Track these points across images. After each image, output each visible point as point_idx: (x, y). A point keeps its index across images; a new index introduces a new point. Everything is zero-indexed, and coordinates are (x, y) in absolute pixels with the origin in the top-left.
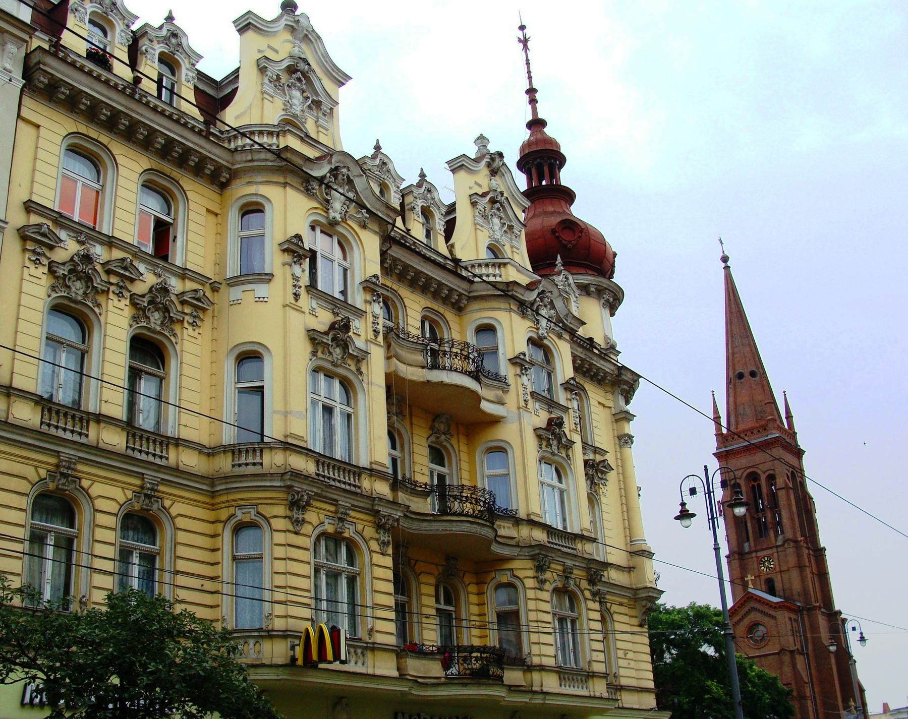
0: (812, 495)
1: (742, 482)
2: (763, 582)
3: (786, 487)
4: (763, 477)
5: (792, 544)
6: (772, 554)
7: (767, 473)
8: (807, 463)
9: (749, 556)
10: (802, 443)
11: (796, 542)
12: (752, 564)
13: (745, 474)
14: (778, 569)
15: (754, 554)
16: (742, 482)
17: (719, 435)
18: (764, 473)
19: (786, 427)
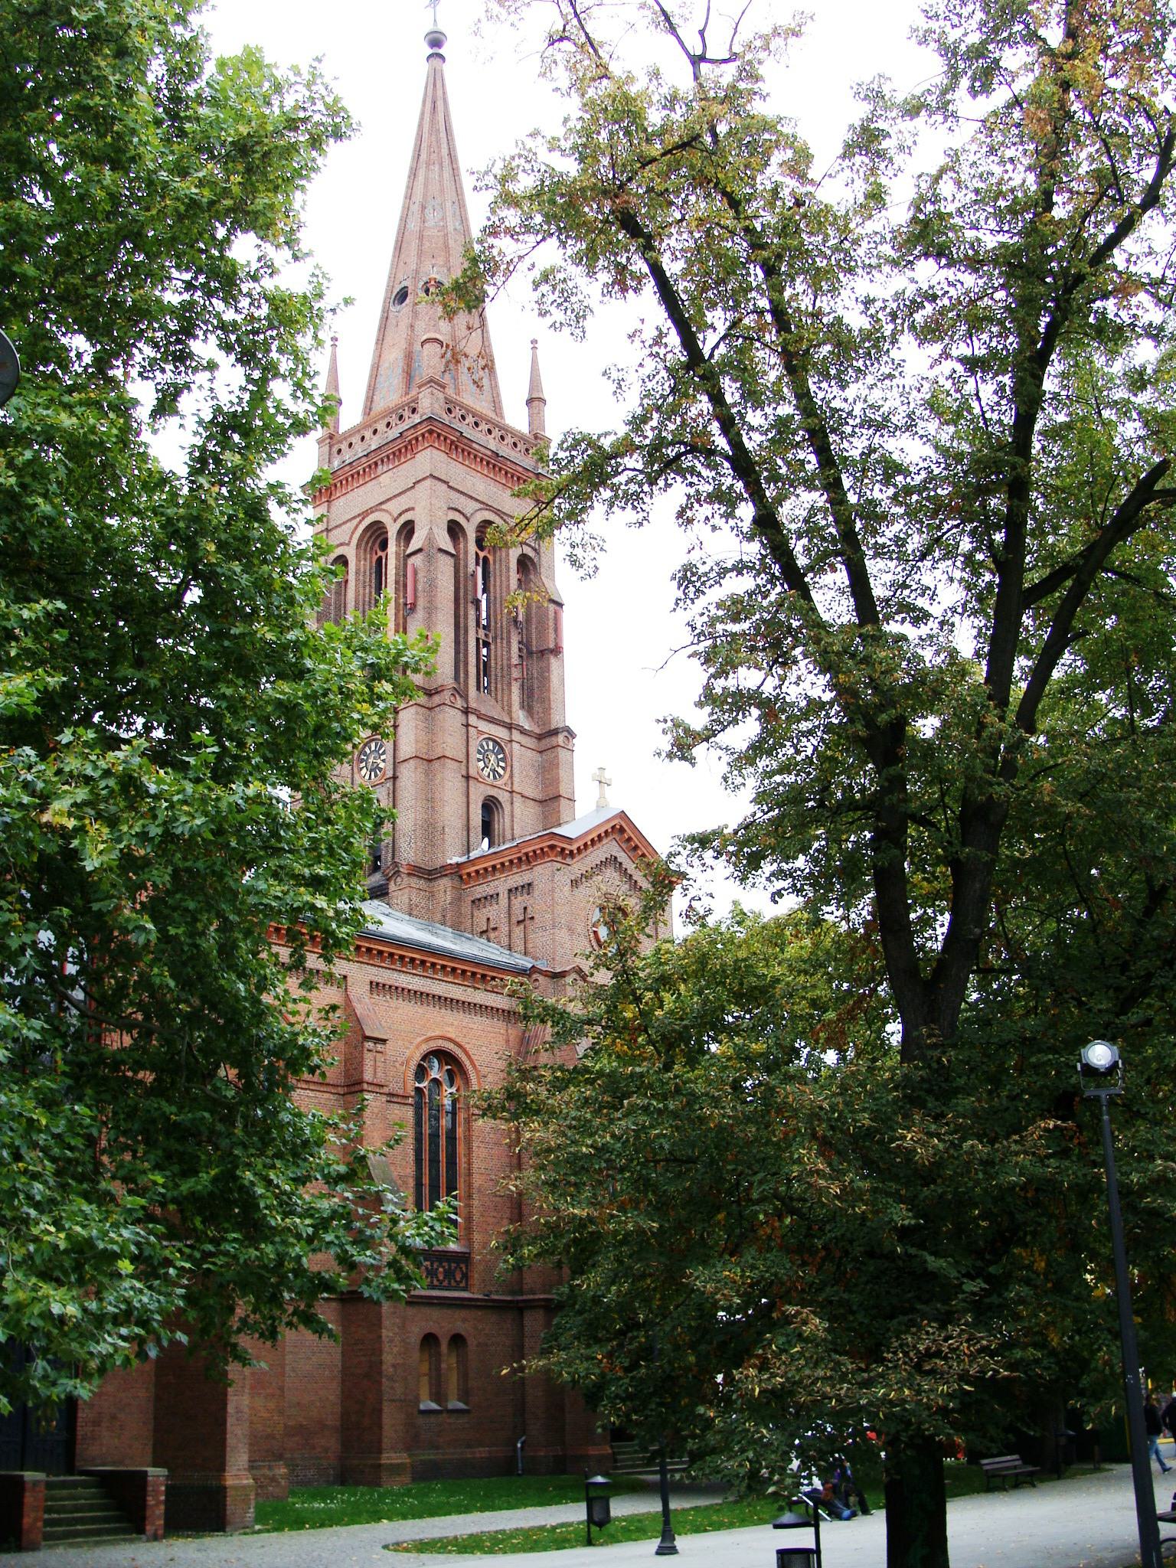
1: (350, 552)
3: (428, 551)
14: (390, 774)
16: (350, 552)
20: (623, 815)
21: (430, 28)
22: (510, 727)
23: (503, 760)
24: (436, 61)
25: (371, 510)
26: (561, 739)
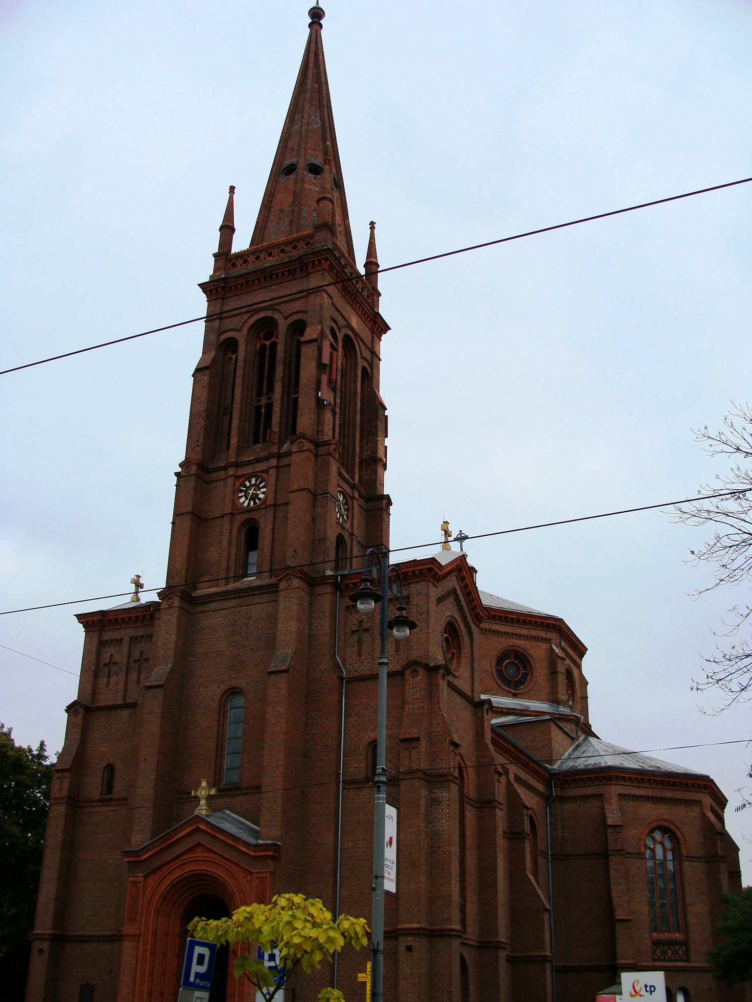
0: (386, 403)
4: (283, 325)
5: (307, 445)
6: (266, 471)
7: (291, 320)
8: (387, 345)
9: (222, 474)
11: (318, 444)
15: (231, 471)
16: (241, 337)
18: (286, 318)
21: (314, 4)
22: (353, 487)
24: (316, 27)
26: (385, 502)
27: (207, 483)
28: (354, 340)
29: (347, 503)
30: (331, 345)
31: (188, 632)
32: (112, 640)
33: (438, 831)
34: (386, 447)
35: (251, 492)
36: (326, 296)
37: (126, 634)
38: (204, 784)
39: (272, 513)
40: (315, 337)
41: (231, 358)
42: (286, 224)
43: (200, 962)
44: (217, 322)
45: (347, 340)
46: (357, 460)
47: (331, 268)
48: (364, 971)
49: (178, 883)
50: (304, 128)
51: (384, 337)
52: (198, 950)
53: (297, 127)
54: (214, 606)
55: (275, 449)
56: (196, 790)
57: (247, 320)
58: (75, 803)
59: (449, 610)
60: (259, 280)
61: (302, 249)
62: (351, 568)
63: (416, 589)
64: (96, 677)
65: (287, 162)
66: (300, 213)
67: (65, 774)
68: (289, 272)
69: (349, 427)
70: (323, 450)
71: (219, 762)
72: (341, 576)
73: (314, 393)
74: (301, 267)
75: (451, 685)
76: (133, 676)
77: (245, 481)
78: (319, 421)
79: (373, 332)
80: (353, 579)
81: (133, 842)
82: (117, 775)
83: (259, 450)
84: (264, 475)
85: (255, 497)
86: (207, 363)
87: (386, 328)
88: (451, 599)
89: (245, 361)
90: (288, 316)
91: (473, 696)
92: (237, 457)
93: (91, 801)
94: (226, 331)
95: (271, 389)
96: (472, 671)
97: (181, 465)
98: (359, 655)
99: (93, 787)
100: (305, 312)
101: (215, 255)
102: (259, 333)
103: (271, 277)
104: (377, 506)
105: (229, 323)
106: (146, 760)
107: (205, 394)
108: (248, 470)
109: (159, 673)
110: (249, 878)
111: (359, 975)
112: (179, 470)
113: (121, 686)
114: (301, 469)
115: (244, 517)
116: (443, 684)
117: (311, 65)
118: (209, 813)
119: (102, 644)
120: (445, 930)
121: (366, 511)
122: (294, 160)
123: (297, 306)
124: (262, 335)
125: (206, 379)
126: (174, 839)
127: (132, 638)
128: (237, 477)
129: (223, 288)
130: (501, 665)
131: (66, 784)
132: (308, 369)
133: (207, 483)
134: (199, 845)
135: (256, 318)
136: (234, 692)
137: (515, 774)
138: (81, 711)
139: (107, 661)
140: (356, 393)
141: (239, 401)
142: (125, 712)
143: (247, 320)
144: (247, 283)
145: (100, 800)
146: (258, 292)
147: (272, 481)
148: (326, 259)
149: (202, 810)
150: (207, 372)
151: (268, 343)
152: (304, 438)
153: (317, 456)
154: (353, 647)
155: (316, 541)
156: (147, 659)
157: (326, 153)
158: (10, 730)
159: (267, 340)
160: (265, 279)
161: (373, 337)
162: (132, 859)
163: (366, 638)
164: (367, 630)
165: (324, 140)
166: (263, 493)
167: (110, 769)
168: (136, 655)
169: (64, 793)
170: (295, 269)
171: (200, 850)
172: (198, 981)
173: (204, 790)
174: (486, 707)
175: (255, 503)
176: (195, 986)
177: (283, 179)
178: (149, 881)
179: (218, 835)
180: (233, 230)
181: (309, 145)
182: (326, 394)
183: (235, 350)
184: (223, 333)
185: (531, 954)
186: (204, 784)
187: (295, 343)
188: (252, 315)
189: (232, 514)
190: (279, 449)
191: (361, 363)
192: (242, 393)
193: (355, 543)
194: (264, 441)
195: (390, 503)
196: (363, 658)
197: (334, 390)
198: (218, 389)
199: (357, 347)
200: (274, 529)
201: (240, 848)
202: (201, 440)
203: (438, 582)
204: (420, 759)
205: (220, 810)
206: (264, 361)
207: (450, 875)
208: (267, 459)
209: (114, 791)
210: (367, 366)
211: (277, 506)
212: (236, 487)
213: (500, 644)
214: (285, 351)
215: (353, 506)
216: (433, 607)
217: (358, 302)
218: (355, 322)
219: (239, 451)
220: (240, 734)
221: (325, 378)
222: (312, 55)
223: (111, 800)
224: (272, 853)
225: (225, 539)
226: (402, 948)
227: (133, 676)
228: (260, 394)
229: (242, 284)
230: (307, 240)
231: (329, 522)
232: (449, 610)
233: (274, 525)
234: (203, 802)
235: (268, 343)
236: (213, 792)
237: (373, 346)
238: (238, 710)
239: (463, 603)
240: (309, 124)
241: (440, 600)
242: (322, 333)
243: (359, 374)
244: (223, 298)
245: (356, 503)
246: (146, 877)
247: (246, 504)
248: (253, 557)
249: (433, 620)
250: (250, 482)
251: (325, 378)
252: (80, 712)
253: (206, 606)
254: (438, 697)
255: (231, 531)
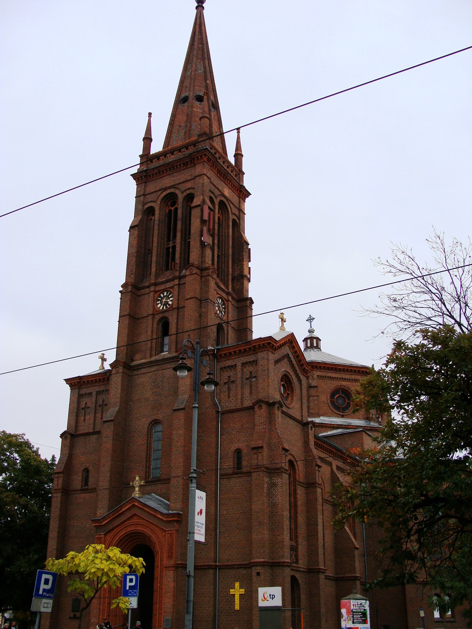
1: (157, 206)
2: (155, 323)
4: (181, 197)
5: (195, 271)
6: (172, 287)
7: (185, 194)
8: (249, 205)
9: (147, 290)
10: (247, 183)
11: (202, 270)
12: (147, 301)
13: (162, 196)
15: (152, 288)
16: (157, 206)
17: (146, 157)
18: (182, 193)
19: (232, 160)
20: (292, 335)
22: (228, 294)
23: (224, 308)
24: (200, 8)
25: (170, 187)
26: (248, 302)
27: (138, 296)
28: (227, 203)
29: (224, 304)
30: (209, 208)
31: (128, 388)
32: (86, 394)
33: (276, 503)
34: (250, 268)
35: (164, 300)
36: (205, 178)
37: (94, 390)
38: (137, 478)
39: (176, 313)
40: (199, 203)
41: (151, 219)
42: (183, 134)
43: (47, 581)
44: (142, 197)
45: (222, 203)
46: (230, 277)
47: (209, 160)
48: (234, 588)
49: (124, 537)
50: (193, 73)
51: (247, 200)
52: (44, 576)
53: (189, 73)
54: (143, 371)
55: (177, 274)
56: (133, 482)
57: (160, 195)
58: (66, 492)
59: (285, 367)
60: (166, 170)
61: (191, 150)
62: (228, 344)
63: (261, 355)
64: (77, 416)
65: (183, 95)
66: (190, 127)
67: (60, 475)
68: (184, 164)
69: (225, 257)
70: (205, 273)
71: (148, 465)
72: (217, 349)
73: (199, 239)
74: (189, 162)
75: (283, 412)
76: (99, 415)
77: (160, 294)
78: (203, 255)
79: (239, 197)
80: (224, 351)
81: (98, 515)
82: (91, 474)
83: (168, 275)
84: (171, 290)
85: (166, 303)
86: (136, 224)
87: (248, 194)
88: (286, 360)
89: (159, 221)
90: (184, 192)
91: (302, 419)
92: (156, 279)
93: (75, 491)
94: (148, 203)
95: (175, 237)
96: (302, 404)
97: (122, 286)
98: (229, 397)
99: (77, 482)
100: (194, 188)
101: (141, 156)
102: (167, 203)
103: (173, 168)
104: (244, 305)
105: (149, 198)
106: (104, 465)
107: (136, 242)
108: (162, 287)
109: (111, 413)
110: (164, 534)
111: (231, 590)
112: (121, 289)
113: (92, 421)
114: (192, 285)
115: (161, 315)
116: (278, 414)
117: (197, 33)
118: (141, 496)
119: (80, 396)
120: (280, 562)
121: (237, 308)
122: (187, 94)
123: (189, 185)
124: (169, 204)
125: (136, 232)
126: (121, 512)
127: (97, 392)
128: (156, 292)
129: (145, 176)
130: (333, 398)
131: (61, 481)
132: (195, 224)
133: (138, 296)
134: (135, 515)
135: (165, 193)
136: (156, 422)
137: (337, 466)
138: (69, 437)
139: (84, 406)
140: (228, 236)
141: (156, 245)
142: (94, 436)
143: (160, 195)
144: (160, 172)
145: (81, 490)
146: (166, 177)
147: (176, 293)
148: (205, 155)
149: (136, 494)
150: (137, 228)
151: (173, 209)
152: (193, 266)
153: (201, 277)
154: (225, 392)
155: (202, 329)
156: (106, 404)
157: (207, 87)
158: (38, 449)
159: (172, 206)
160: (170, 169)
161: (239, 200)
162: (97, 524)
163: (233, 387)
164: (233, 382)
165: (206, 80)
166: (171, 301)
167: (86, 471)
168: (100, 402)
169: (60, 486)
170: (187, 162)
171: (136, 518)
172: (45, 594)
173: (137, 481)
174: (310, 426)
175: (166, 307)
176: (42, 596)
177: (180, 106)
178: (107, 537)
179: (145, 509)
180: (151, 140)
181: (196, 84)
182: (207, 239)
183: (154, 214)
184: (146, 204)
185: (347, 575)
186: (137, 478)
187: (188, 208)
188: (163, 192)
189: (153, 314)
190: (180, 273)
191: (231, 217)
192: (158, 240)
193: (230, 328)
194: (171, 269)
195: (252, 302)
196: (231, 399)
197: (213, 236)
198: (144, 238)
199: (229, 208)
200: (177, 323)
201: (158, 516)
202: (134, 270)
203: (275, 350)
204: (263, 459)
205: (149, 494)
206: (170, 219)
207: (283, 529)
208: (173, 280)
209: (89, 484)
210: (236, 219)
211: (179, 308)
212: (155, 298)
213: (333, 385)
214: (182, 213)
215: (228, 306)
216: (271, 366)
217: (228, 180)
218: (227, 192)
219: (157, 275)
220: (160, 448)
221: (205, 229)
222: (198, 27)
223: (87, 489)
224: (176, 519)
225: (150, 330)
226: (254, 574)
227: (99, 415)
228: (169, 240)
229: (156, 173)
230: (194, 144)
231: (209, 317)
232: (285, 367)
233: (177, 320)
234: (137, 489)
235: (173, 209)
236: (142, 483)
237: (240, 206)
238: (159, 433)
239: (294, 362)
240: (196, 70)
241: (277, 362)
242: (204, 201)
243: (231, 224)
244: (146, 183)
245: (229, 303)
246: (105, 535)
247: (161, 308)
248: (167, 340)
249: (272, 374)
250: (163, 294)
251: (205, 229)
252: (69, 437)
253: (139, 371)
254: (275, 421)
255: (153, 325)
